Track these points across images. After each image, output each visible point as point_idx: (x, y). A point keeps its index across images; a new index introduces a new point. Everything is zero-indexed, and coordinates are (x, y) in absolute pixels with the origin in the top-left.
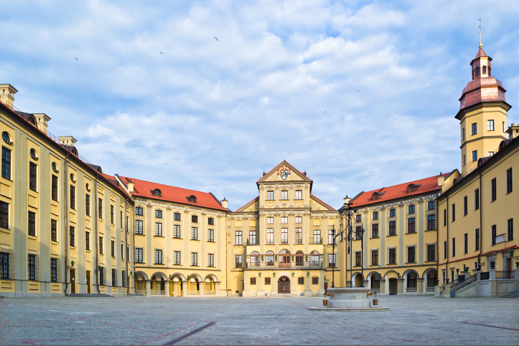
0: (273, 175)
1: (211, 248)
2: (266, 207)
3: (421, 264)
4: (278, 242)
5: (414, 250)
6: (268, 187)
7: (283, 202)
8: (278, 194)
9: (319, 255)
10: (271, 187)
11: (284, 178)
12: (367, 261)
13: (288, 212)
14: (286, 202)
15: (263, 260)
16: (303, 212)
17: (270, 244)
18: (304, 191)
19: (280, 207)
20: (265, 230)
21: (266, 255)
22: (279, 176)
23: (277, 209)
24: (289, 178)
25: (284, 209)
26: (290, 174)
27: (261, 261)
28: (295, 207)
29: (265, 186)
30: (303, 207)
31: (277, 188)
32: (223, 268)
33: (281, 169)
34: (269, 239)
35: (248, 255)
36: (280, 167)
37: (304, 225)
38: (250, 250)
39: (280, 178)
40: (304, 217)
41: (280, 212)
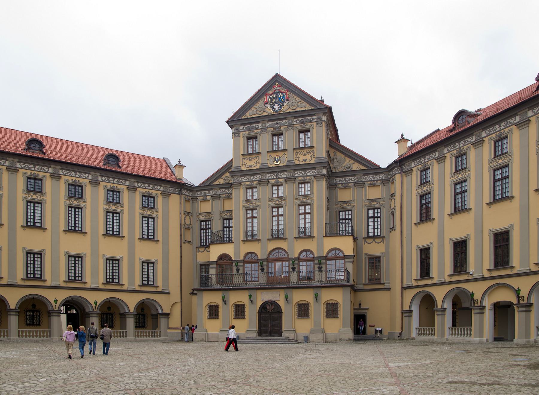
0: (257, 105)
1: (147, 251)
2: (243, 168)
3: (526, 269)
4: (264, 235)
5: (508, 240)
6: (248, 129)
7: (273, 155)
8: (264, 142)
9: (345, 257)
10: (254, 129)
11: (277, 107)
12: (442, 264)
13: (284, 175)
14: (281, 154)
15: (238, 270)
16: (312, 173)
17: (251, 238)
18: (314, 131)
19: (270, 166)
20: (241, 212)
21: (244, 262)
22: (269, 106)
23: (265, 170)
24: (285, 108)
25: (277, 170)
26: (287, 100)
27: (235, 272)
28: (297, 163)
29: (241, 128)
30: (313, 161)
31: (264, 129)
32: (174, 286)
33: (271, 92)
34: (250, 229)
35: (213, 263)
36: (268, 90)
37: (315, 199)
38: (215, 252)
39: (269, 110)
40: (315, 184)
41: (269, 176)
